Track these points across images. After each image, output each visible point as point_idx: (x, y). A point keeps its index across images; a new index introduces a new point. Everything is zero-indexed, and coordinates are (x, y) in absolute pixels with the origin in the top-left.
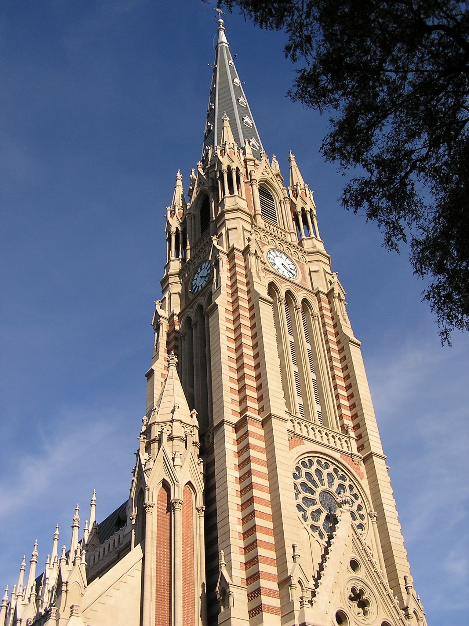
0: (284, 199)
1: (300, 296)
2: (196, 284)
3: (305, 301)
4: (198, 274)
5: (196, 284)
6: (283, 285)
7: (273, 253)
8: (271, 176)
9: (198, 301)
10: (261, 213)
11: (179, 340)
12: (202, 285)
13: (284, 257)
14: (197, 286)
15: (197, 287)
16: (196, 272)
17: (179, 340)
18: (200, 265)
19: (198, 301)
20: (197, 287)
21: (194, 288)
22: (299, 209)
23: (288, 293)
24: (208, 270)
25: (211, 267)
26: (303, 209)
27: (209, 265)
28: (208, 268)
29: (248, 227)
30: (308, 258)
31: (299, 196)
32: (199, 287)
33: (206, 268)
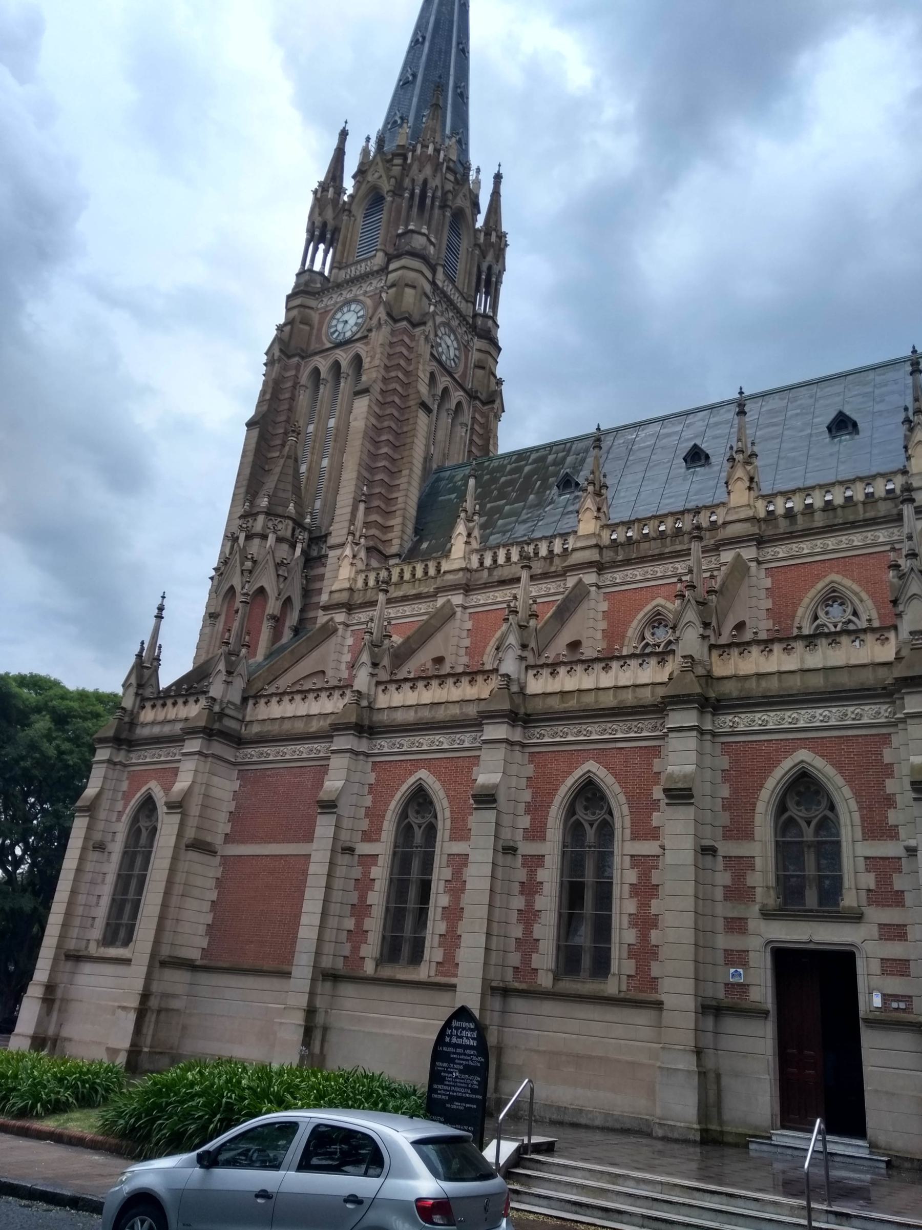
6: (444, 379)
7: (442, 329)
13: (452, 337)
14: (336, 330)
15: (337, 333)
16: (340, 309)
18: (348, 303)
19: (337, 356)
20: (337, 333)
21: (332, 330)
23: (446, 390)
24: (358, 318)
25: (363, 315)
26: (490, 268)
29: (428, 288)
33: (357, 313)
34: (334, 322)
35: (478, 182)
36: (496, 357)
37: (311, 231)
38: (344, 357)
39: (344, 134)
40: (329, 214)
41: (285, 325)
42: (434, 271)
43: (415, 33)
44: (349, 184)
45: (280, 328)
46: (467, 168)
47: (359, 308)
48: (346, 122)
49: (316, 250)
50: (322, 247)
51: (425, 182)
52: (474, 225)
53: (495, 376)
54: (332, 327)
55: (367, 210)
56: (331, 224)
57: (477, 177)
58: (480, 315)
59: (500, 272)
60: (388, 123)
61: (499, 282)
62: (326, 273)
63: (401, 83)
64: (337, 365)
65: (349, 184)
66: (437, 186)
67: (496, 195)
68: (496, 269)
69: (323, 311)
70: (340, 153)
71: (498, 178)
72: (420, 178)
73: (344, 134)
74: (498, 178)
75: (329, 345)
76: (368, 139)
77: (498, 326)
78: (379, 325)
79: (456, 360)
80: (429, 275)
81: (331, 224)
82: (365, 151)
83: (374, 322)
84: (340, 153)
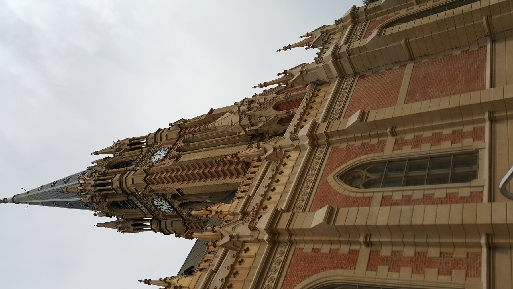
0: (120, 156)
1: (180, 144)
2: (167, 210)
3: (183, 142)
4: (161, 208)
5: (167, 210)
7: (152, 160)
8: (105, 163)
9: (177, 206)
10: (126, 168)
11: (201, 221)
12: (167, 205)
14: (168, 209)
15: (169, 209)
16: (160, 210)
17: (201, 221)
19: (177, 206)
20: (169, 209)
21: (169, 211)
22: (128, 147)
25: (156, 199)
26: (128, 145)
27: (156, 200)
28: (157, 201)
29: (133, 172)
30: (159, 141)
31: (120, 147)
32: (169, 208)
34: (166, 211)
35: (97, 162)
36: (162, 130)
37: (138, 230)
38: (177, 203)
39: (99, 225)
40: (129, 224)
41: (176, 233)
42: (128, 171)
43: (53, 206)
44: (114, 219)
45: (178, 235)
46: (90, 168)
47: (155, 202)
48: (95, 225)
49: (146, 225)
50: (144, 223)
51: (93, 186)
52: (113, 158)
53: (170, 128)
54: (168, 211)
55: (122, 209)
56: (131, 222)
57: (95, 162)
58: (147, 144)
59: (129, 140)
60: (87, 208)
61: (134, 139)
62: (151, 219)
63: (73, 207)
64: (180, 205)
65: (114, 219)
66: (94, 180)
67: (102, 152)
68: (128, 142)
69: (165, 217)
70: (106, 225)
71: (96, 153)
72: (93, 189)
73: (99, 225)
74: (96, 153)
75: (176, 212)
76: (95, 215)
77: (150, 134)
78: (152, 191)
79: (166, 149)
80: (128, 172)
81: (131, 222)
82: (99, 215)
83: (151, 194)
84: (106, 225)
